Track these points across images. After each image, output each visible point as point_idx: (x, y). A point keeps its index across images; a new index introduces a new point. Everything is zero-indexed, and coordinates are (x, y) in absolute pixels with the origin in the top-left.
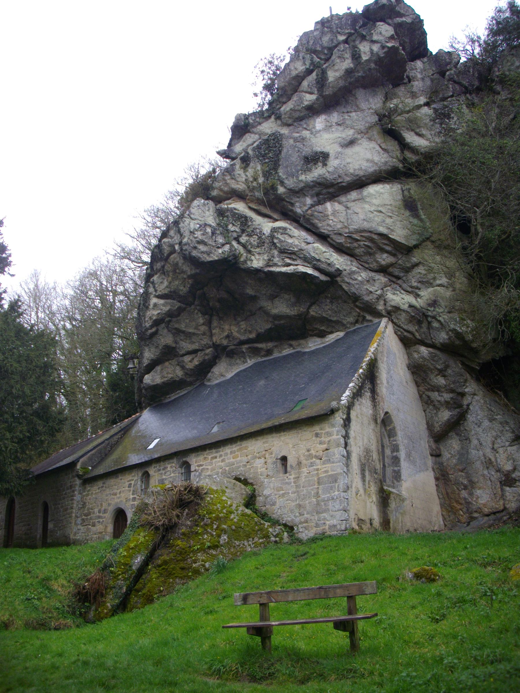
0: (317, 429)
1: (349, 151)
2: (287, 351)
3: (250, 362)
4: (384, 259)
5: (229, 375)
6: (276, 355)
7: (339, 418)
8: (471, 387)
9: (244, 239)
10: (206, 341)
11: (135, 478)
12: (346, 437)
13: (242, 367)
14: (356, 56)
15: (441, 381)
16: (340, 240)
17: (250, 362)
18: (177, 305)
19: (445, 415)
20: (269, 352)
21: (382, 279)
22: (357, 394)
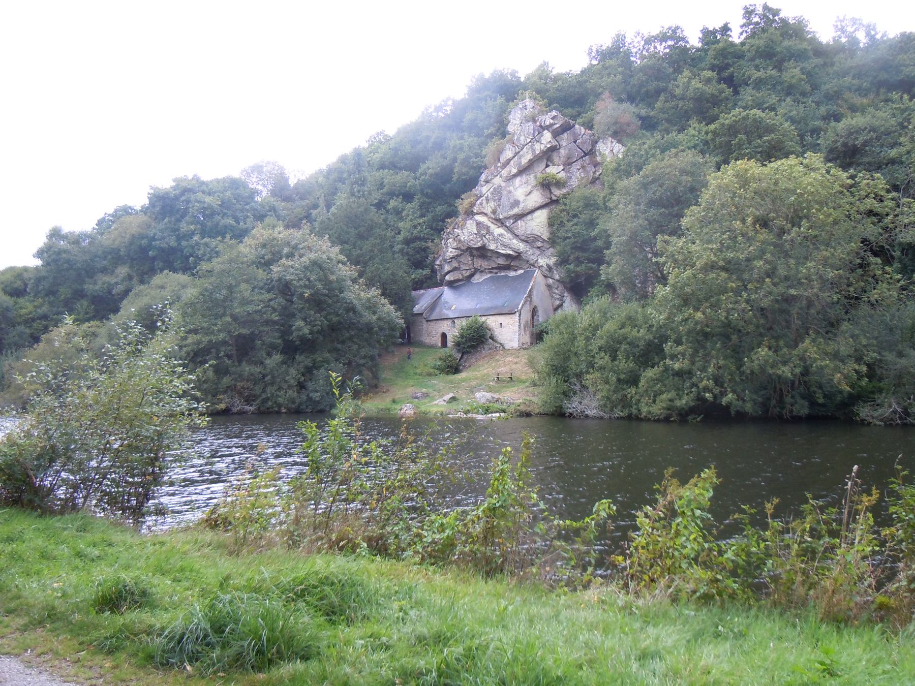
0: (511, 316)
1: (529, 197)
2: (503, 274)
3: (489, 276)
4: (539, 244)
5: (481, 280)
6: (499, 274)
7: (517, 314)
8: (566, 295)
9: (487, 236)
10: (471, 266)
11: (449, 322)
12: (520, 320)
13: (486, 277)
14: (534, 151)
15: (557, 291)
16: (523, 238)
17: (489, 276)
18: (460, 252)
19: (558, 303)
20: (496, 273)
21: (538, 252)
22: (525, 302)
